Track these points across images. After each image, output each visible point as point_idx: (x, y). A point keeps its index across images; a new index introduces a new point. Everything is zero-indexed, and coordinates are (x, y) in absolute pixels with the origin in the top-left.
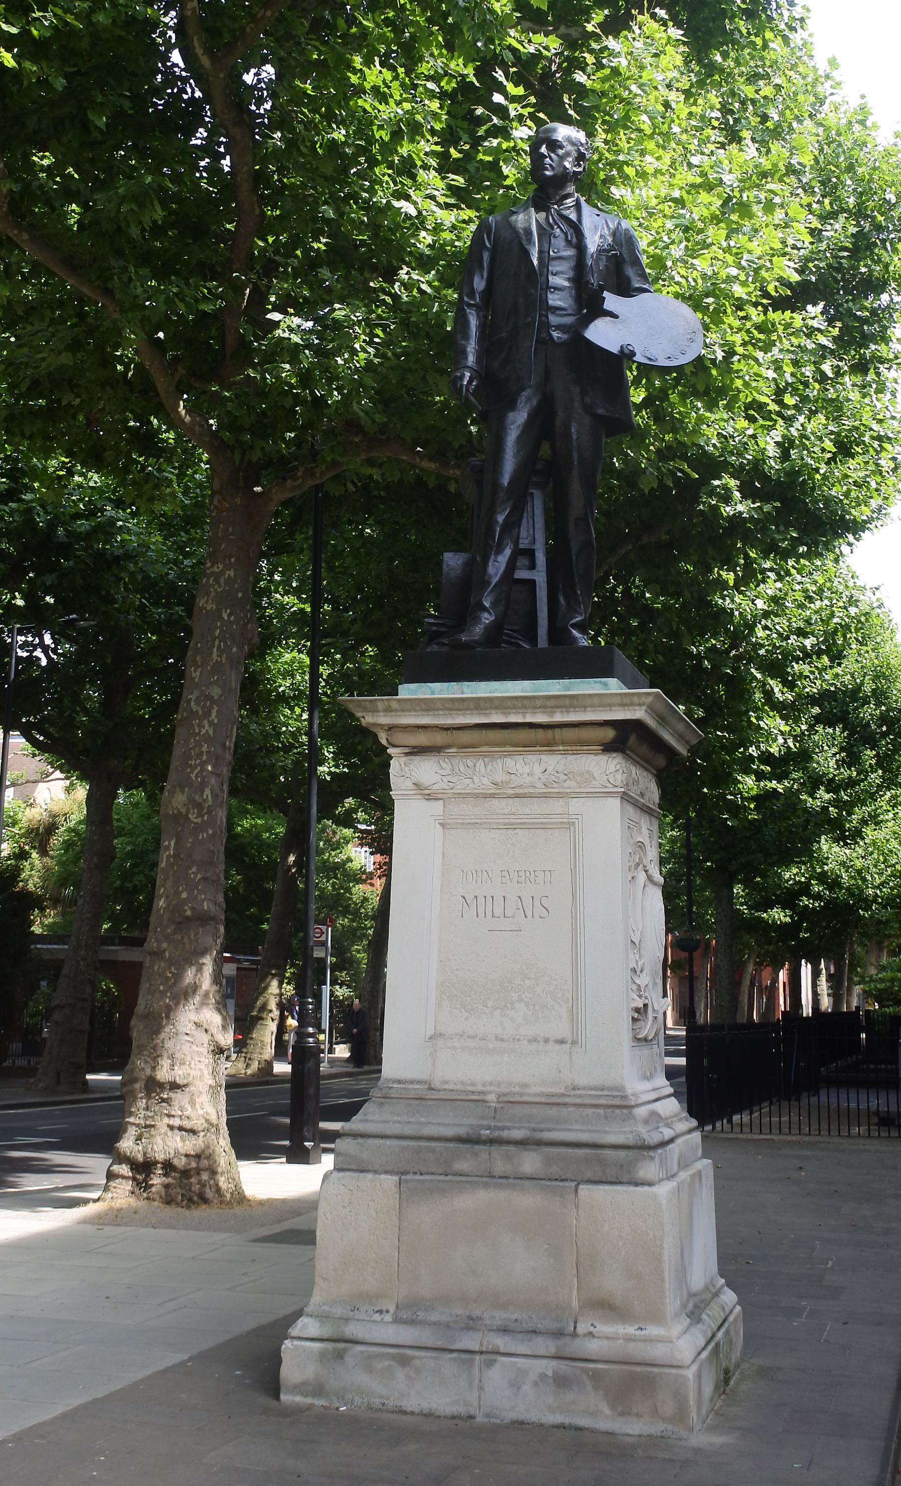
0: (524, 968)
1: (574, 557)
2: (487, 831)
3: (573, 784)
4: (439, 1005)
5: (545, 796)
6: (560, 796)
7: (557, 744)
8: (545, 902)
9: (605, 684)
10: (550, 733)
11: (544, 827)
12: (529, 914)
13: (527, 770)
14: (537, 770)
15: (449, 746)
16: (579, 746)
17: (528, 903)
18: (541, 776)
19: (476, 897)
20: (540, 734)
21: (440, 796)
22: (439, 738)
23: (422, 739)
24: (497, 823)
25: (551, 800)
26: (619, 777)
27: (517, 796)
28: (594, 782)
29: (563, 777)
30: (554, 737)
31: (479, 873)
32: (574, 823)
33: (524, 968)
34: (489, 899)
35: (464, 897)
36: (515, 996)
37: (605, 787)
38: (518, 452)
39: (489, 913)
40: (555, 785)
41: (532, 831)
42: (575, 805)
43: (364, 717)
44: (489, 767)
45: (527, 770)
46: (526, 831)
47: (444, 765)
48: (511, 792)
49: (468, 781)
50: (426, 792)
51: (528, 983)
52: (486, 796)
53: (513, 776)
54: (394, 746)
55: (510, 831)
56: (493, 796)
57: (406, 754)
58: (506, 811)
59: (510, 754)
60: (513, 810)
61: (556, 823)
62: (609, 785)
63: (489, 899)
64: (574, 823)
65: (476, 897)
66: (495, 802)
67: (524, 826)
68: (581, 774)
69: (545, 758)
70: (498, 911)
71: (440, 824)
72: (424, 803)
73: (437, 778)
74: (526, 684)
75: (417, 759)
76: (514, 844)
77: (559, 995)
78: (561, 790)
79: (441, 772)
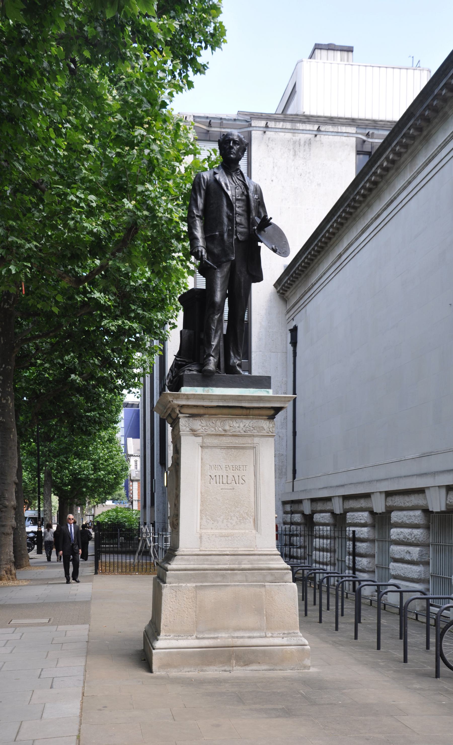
3: (255, 431)
4: (201, 519)
6: (250, 436)
7: (250, 415)
8: (244, 478)
9: (268, 392)
10: (248, 411)
12: (237, 482)
13: (237, 425)
14: (242, 425)
15: (205, 414)
16: (259, 416)
17: (237, 478)
19: (215, 476)
20: (244, 411)
21: (201, 435)
22: (202, 411)
23: (195, 411)
25: (247, 438)
29: (252, 429)
30: (250, 412)
31: (217, 466)
32: (255, 447)
34: (221, 477)
35: (210, 476)
36: (232, 514)
39: (221, 482)
40: (249, 432)
41: (238, 450)
42: (256, 440)
43: (172, 401)
45: (237, 425)
46: (236, 450)
48: (230, 434)
49: (213, 429)
52: (220, 435)
54: (181, 413)
56: (223, 435)
58: (228, 442)
63: (221, 477)
64: (255, 447)
65: (215, 476)
66: (224, 438)
67: (235, 448)
69: (244, 421)
70: (225, 481)
72: (194, 438)
73: (200, 427)
78: (251, 434)
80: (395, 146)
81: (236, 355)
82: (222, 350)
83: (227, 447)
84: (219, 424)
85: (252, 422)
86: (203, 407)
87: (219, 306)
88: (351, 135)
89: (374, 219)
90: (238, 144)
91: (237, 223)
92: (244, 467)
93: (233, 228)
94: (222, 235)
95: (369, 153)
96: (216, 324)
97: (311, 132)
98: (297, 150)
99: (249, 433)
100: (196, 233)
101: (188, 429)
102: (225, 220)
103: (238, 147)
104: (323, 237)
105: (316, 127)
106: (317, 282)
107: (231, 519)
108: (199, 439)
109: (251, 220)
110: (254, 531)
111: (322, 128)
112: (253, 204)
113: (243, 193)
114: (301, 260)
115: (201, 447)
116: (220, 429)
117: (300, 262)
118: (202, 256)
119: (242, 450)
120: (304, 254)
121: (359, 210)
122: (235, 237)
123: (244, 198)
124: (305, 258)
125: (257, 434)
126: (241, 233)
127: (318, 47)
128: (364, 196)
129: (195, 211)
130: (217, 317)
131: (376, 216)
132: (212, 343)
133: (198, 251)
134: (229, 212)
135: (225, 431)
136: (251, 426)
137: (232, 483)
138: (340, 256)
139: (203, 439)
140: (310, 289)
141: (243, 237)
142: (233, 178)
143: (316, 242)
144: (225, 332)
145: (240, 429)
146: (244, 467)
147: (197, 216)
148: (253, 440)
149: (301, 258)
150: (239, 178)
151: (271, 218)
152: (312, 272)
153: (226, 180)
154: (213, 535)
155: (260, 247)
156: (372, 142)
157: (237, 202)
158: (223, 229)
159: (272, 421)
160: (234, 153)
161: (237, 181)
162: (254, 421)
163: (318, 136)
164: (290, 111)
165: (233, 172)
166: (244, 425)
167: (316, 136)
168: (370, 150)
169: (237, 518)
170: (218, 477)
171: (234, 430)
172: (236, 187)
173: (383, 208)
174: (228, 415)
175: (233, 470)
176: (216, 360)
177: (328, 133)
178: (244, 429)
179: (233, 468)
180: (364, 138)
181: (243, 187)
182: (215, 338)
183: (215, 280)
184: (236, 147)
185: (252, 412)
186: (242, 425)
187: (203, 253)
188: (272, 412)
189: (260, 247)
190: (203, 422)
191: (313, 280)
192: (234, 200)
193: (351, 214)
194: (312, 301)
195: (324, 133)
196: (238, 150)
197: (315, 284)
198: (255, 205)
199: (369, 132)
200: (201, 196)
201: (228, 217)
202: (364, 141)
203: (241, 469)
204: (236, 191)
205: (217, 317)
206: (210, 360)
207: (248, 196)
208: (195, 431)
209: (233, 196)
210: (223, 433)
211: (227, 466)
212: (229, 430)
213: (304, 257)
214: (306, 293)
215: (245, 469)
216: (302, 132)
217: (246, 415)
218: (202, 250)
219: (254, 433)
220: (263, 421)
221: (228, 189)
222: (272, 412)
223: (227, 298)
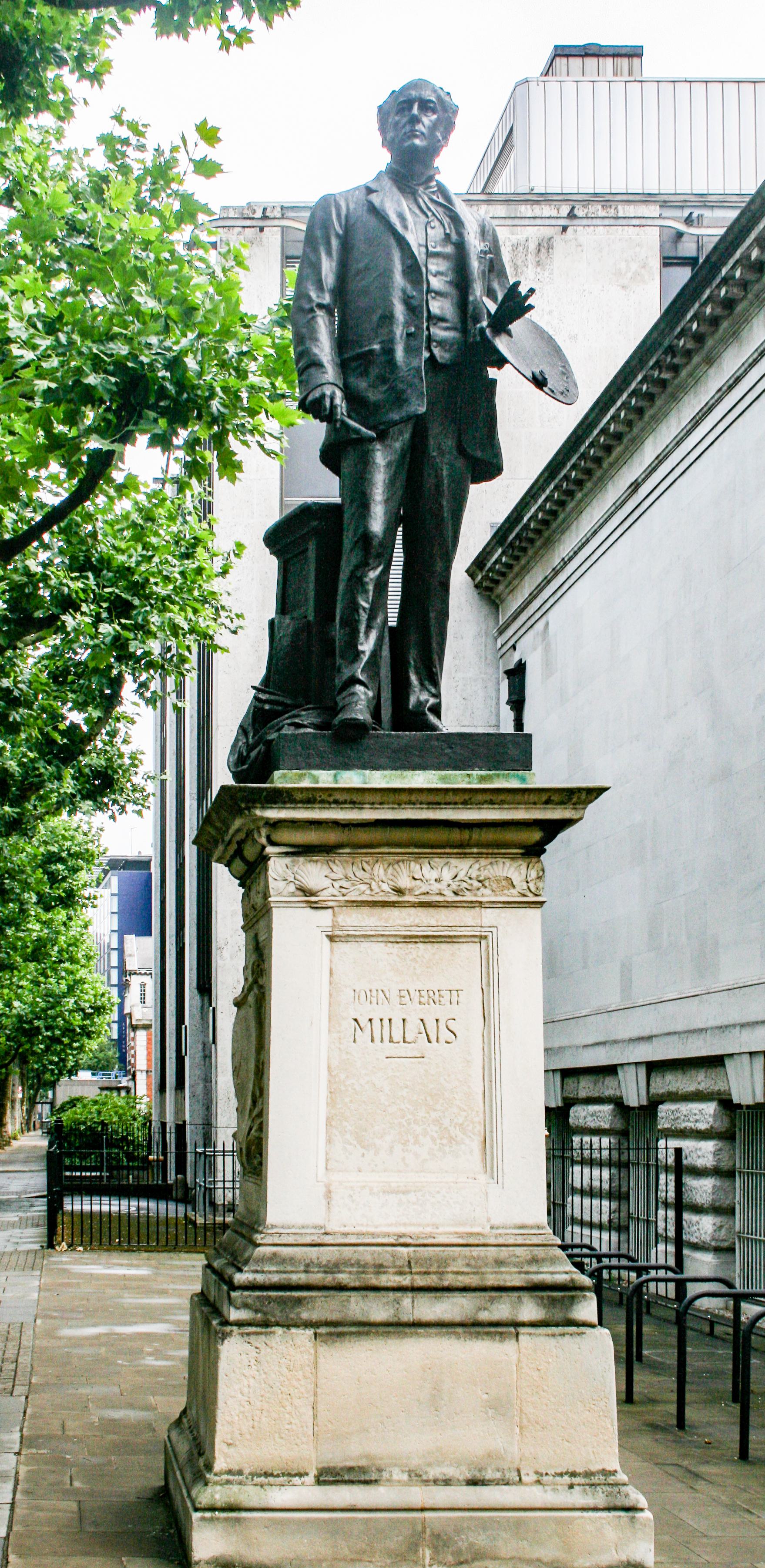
0: (429, 1098)
2: (383, 945)
3: (487, 892)
4: (329, 1141)
7: (469, 846)
10: (466, 834)
12: (433, 1038)
13: (434, 874)
14: (447, 875)
15: (341, 846)
18: (451, 882)
20: (456, 835)
21: (330, 904)
22: (331, 837)
23: (311, 837)
24: (396, 936)
25: (461, 910)
28: (512, 891)
29: (476, 884)
30: (471, 838)
31: (374, 993)
33: (429, 1098)
34: (386, 1023)
35: (356, 1020)
37: (524, 896)
41: (436, 945)
42: (489, 916)
45: (434, 874)
46: (429, 946)
47: (335, 868)
48: (412, 899)
49: (363, 887)
50: (313, 899)
51: (434, 1115)
52: (385, 904)
53: (418, 882)
57: (287, 854)
58: (408, 922)
59: (418, 857)
62: (529, 894)
63: (386, 1023)
64: (486, 937)
65: (370, 1020)
66: (395, 912)
67: (427, 939)
68: (498, 881)
69: (454, 862)
70: (397, 1035)
71: (327, 936)
73: (327, 883)
76: (414, 960)
77: (470, 1128)
78: (474, 899)
80: (748, 248)
81: (426, 683)
82: (385, 671)
84: (382, 871)
85: (477, 866)
86: (336, 824)
87: (381, 544)
88: (649, 222)
89: (725, 388)
90: (434, 111)
91: (431, 317)
92: (454, 993)
93: (419, 328)
94: (389, 351)
95: (691, 262)
96: (371, 593)
97: (553, 222)
98: (519, 263)
99: (469, 897)
100: (316, 351)
101: (292, 888)
102: (399, 311)
103: (434, 117)
104: (592, 445)
105: (565, 210)
106: (576, 553)
107: (416, 1142)
108: (325, 917)
109: (471, 308)
110: (483, 1178)
111: (580, 212)
112: (475, 265)
113: (447, 236)
114: (536, 506)
115: (331, 938)
116: (385, 887)
117: (533, 510)
118: (333, 407)
119: (449, 945)
120: (544, 491)
121: (684, 373)
122: (426, 355)
123: (449, 249)
124: (547, 499)
126: (441, 343)
127: (562, 52)
128: (699, 338)
129: (313, 295)
130: (373, 574)
131: (731, 382)
132: (360, 648)
133: (323, 396)
134: (409, 288)
135: (399, 891)
136: (474, 876)
137: (419, 1041)
138: (635, 486)
139: (334, 915)
140: (556, 572)
141: (447, 356)
142: (421, 201)
143: (573, 460)
144: (393, 622)
145: (442, 886)
146: (454, 993)
147: (320, 306)
149: (536, 502)
150: (435, 197)
151: (532, 291)
152: (563, 532)
153: (399, 205)
154: (364, 1187)
155: (494, 382)
156: (698, 236)
157: (431, 260)
158: (391, 332)
159: (534, 860)
160: (422, 133)
161: (432, 207)
162: (483, 862)
163: (570, 230)
164: (501, 186)
165: (420, 185)
167: (565, 229)
168: (693, 254)
169: (433, 1140)
170: (376, 1023)
171: (425, 889)
172: (428, 223)
173: (751, 360)
174: (407, 846)
175: (420, 1003)
176: (371, 694)
177: (595, 222)
178: (454, 886)
179: (421, 996)
180: (682, 227)
181: (446, 221)
182: (367, 634)
183: (370, 473)
184: (428, 120)
185: (477, 835)
186: (447, 875)
187: (338, 401)
188: (536, 836)
189: (494, 382)
190: (335, 868)
191: (564, 548)
192: (424, 256)
193: (663, 384)
194: (562, 600)
195: (585, 222)
196: (434, 127)
197: (571, 559)
198: (482, 268)
199: (691, 214)
200: (329, 253)
201: (407, 301)
202: (680, 235)
203: (445, 1000)
204: (429, 230)
205: (373, 574)
206: (353, 694)
207: (461, 248)
208: (312, 894)
209: (420, 245)
210: (394, 898)
211: (403, 993)
212: (411, 890)
213: (543, 497)
214: (548, 581)
215: (454, 1000)
216: (532, 222)
217: (461, 846)
218: (334, 393)
219: (483, 895)
220: (508, 862)
221: (406, 227)
222: (536, 836)
223: (400, 529)
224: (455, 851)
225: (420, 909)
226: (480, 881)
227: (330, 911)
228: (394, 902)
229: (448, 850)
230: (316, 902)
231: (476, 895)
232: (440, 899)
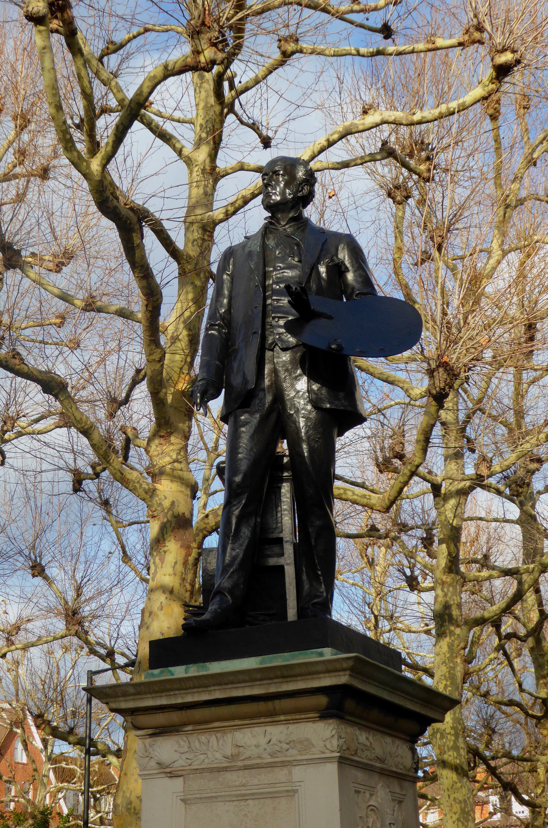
1: (313, 541)
2: (222, 804)
3: (294, 752)
5: (271, 766)
6: (284, 764)
10: (270, 705)
11: (273, 796)
13: (254, 742)
14: (263, 741)
15: (185, 724)
18: (266, 746)
20: (261, 706)
24: (230, 795)
26: (335, 742)
27: (246, 768)
28: (313, 749)
29: (285, 746)
37: (323, 753)
38: (251, 449)
40: (279, 754)
41: (262, 801)
42: (298, 773)
44: (221, 742)
46: (256, 802)
47: (182, 743)
48: (240, 764)
49: (202, 757)
50: (168, 770)
53: (241, 749)
55: (242, 803)
56: (225, 769)
58: (237, 783)
59: (239, 727)
60: (244, 781)
61: (282, 792)
62: (327, 751)
64: (297, 790)
67: (254, 796)
68: (301, 742)
69: (270, 729)
71: (182, 800)
72: (167, 782)
73: (176, 756)
74: (259, 658)
75: (160, 740)
76: (246, 815)
79: (182, 750)
83: (237, 796)
125: (299, 758)
136: (282, 739)
139: (185, 783)
148: (290, 773)
166: (267, 739)
185: (279, 704)
212: (238, 755)
224: (268, 720)
225: (247, 771)
226: (288, 744)
227: (181, 779)
228: (226, 767)
229: (262, 720)
230: (170, 773)
231: (286, 756)
232: (259, 761)
